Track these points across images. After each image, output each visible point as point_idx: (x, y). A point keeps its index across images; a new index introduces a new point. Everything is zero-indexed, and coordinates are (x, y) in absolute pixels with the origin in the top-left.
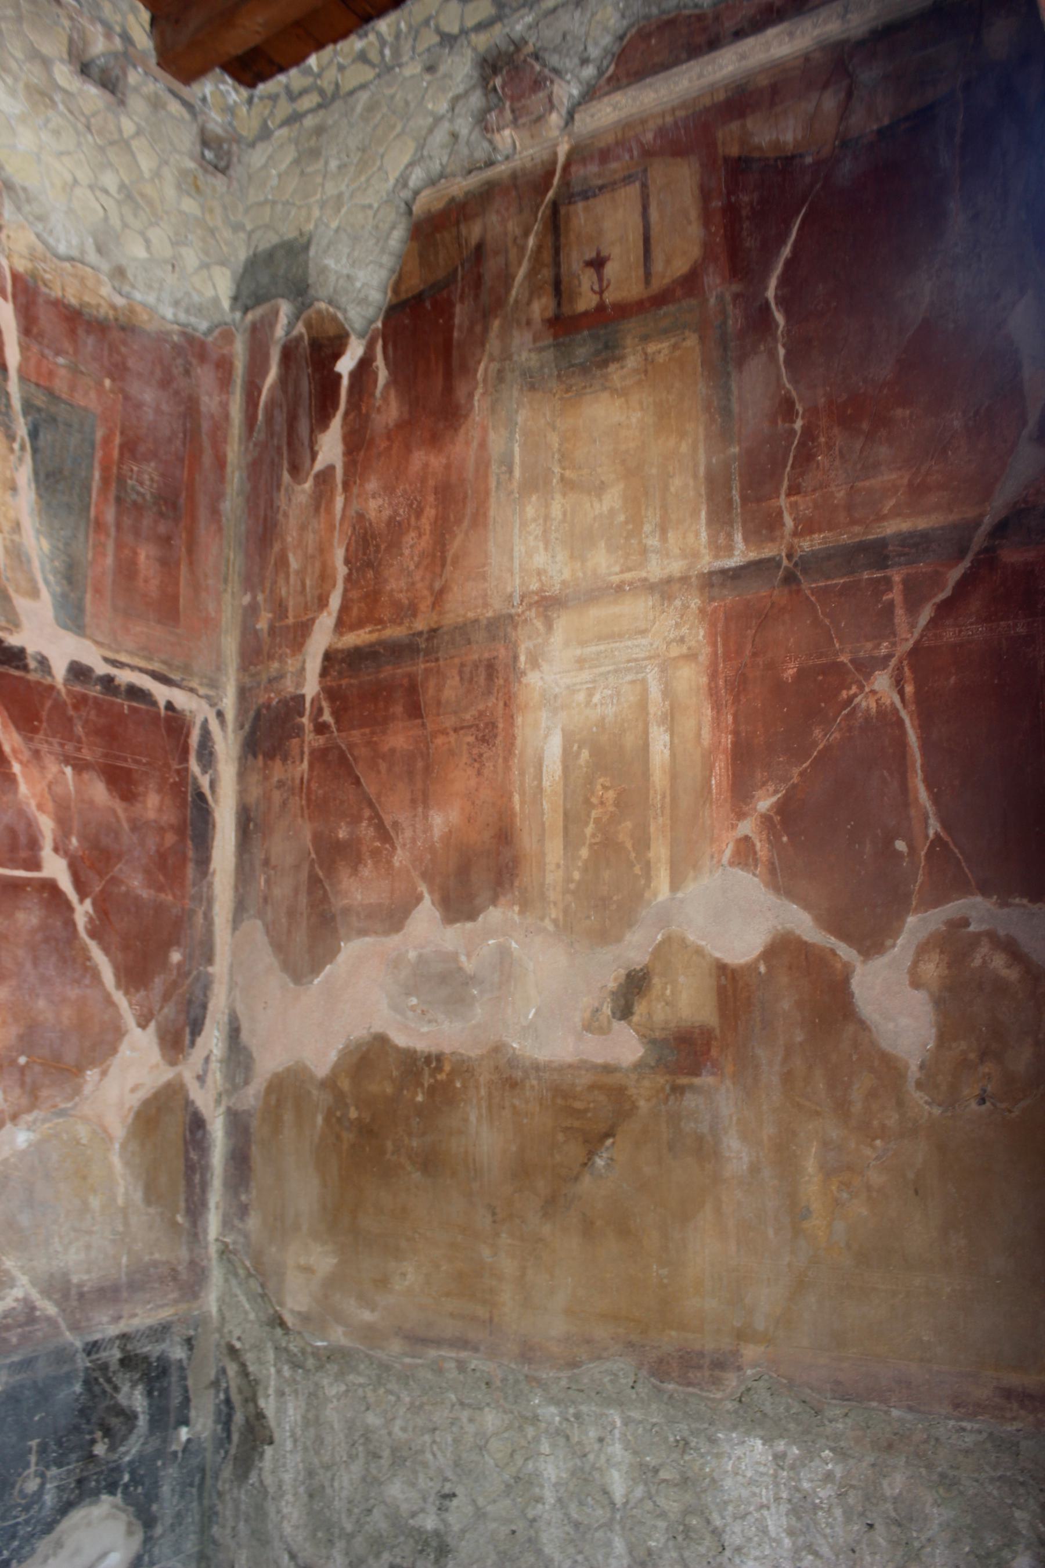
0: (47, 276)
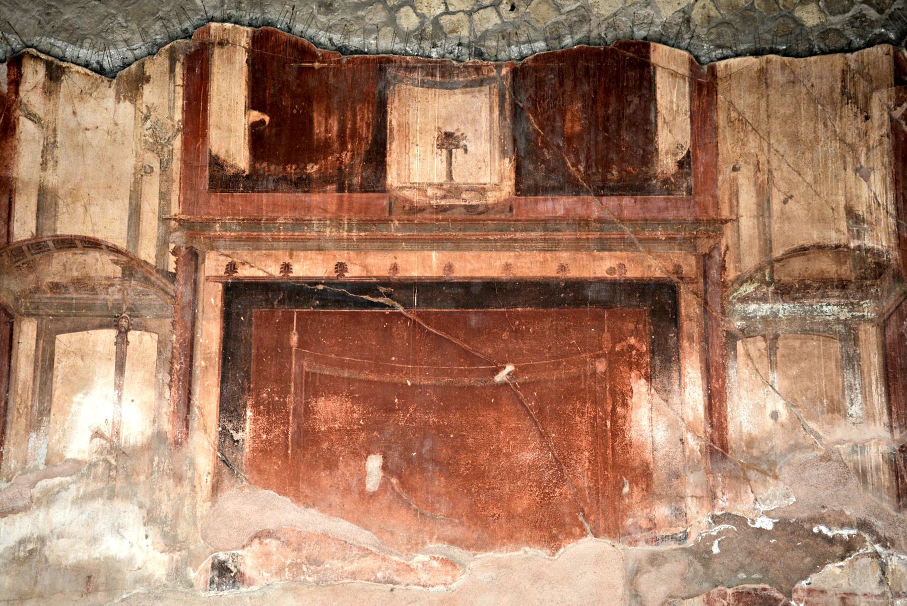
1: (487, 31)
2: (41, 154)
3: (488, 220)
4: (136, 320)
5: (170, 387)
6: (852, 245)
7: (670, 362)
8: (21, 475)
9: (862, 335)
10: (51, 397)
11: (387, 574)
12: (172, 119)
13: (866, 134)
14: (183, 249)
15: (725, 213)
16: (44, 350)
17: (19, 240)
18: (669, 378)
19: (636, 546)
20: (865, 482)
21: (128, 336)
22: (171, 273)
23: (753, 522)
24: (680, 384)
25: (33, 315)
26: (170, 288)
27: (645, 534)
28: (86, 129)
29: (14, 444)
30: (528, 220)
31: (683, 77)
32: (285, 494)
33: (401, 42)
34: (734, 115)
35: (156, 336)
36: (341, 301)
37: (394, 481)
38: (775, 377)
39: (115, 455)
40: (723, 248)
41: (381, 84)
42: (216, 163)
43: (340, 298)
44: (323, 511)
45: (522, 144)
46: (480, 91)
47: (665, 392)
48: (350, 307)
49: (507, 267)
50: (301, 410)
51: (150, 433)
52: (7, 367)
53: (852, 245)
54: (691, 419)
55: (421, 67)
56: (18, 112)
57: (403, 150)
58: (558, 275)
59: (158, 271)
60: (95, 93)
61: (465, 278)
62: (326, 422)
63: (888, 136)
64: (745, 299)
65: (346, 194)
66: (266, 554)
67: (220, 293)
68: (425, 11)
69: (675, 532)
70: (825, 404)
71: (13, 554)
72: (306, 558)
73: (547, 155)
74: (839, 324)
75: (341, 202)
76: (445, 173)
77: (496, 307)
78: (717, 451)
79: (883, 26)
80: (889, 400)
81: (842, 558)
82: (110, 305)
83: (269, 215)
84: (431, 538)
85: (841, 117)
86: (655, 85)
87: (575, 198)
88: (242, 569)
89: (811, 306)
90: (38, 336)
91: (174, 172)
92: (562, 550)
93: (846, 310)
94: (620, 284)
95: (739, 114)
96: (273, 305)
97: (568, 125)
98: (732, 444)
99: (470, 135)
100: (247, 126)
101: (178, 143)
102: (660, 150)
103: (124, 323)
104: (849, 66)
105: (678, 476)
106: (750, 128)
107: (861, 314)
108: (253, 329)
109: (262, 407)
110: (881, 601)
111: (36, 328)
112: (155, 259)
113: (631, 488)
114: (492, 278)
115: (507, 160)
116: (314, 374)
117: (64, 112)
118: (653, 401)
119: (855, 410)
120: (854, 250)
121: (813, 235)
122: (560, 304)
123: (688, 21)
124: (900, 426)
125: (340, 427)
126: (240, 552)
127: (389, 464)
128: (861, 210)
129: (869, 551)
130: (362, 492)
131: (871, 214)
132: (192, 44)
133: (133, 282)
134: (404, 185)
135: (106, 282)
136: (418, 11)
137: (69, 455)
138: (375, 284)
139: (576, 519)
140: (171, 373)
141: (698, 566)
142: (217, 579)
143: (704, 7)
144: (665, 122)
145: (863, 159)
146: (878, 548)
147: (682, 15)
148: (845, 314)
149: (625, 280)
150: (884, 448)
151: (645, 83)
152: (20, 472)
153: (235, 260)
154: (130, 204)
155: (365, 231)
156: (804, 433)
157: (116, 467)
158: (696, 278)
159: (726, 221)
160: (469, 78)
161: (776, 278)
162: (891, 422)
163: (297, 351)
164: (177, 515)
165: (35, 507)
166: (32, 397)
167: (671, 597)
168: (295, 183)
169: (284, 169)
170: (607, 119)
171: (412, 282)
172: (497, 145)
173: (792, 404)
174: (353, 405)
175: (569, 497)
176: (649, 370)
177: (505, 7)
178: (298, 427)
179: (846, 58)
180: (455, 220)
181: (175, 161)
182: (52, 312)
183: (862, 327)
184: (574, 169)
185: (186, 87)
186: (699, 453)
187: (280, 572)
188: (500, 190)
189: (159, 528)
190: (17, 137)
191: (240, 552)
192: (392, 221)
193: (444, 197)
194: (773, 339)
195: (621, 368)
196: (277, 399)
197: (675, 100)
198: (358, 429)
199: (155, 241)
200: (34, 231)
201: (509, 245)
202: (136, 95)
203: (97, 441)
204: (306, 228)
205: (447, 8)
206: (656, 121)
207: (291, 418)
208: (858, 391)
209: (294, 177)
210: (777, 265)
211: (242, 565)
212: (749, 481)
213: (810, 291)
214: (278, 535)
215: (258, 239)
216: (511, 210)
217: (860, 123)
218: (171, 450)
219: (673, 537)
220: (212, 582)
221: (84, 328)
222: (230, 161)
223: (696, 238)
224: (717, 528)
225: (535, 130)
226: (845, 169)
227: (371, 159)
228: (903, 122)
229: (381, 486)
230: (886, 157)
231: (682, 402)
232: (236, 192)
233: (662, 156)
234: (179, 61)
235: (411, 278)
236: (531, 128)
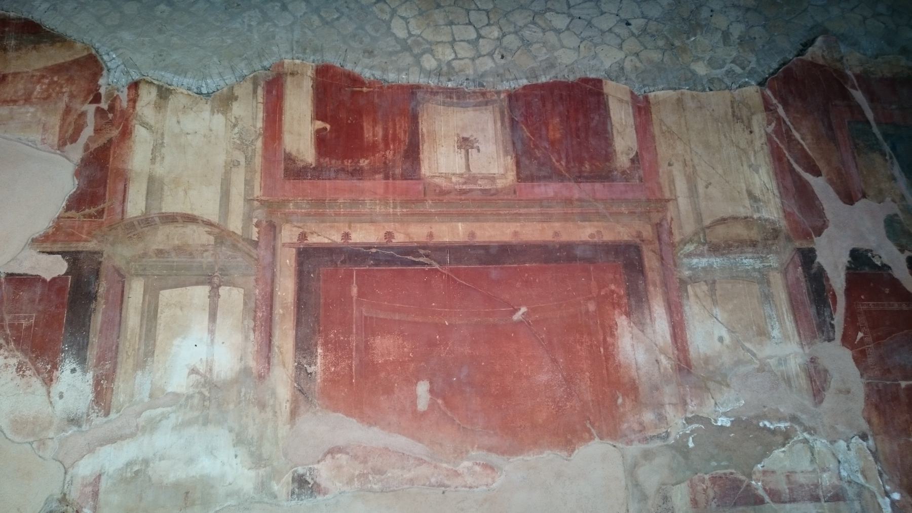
0: (872, 69)
1: (486, 71)
2: (151, 152)
3: (499, 200)
5: (254, 331)
6: (755, 216)
7: (642, 302)
8: (128, 407)
9: (772, 279)
10: (155, 341)
11: (439, 479)
12: (255, 126)
13: (752, 142)
14: (264, 223)
15: (667, 195)
16: (150, 303)
18: (643, 313)
19: (631, 445)
20: (790, 386)
22: (254, 241)
23: (716, 421)
24: (651, 319)
25: (141, 275)
26: (254, 252)
27: (638, 435)
28: (188, 134)
29: (123, 381)
30: (527, 200)
31: (627, 102)
32: (352, 416)
33: (424, 77)
34: (664, 128)
35: (242, 291)
36: (391, 261)
37: (440, 401)
38: (717, 311)
39: (208, 388)
40: (669, 219)
41: (413, 104)
42: (289, 159)
43: (389, 258)
44: (383, 429)
45: (519, 146)
46: (486, 109)
47: (641, 325)
48: (398, 265)
49: (516, 234)
50: (362, 347)
51: (238, 369)
52: (118, 317)
53: (755, 216)
54: (662, 344)
55: (442, 92)
56: (134, 121)
57: (432, 151)
58: (553, 239)
59: (244, 240)
60: (195, 108)
61: (484, 242)
62: (382, 356)
63: (766, 144)
64: (689, 255)
65: (391, 181)
66: (338, 467)
68: (441, 57)
69: (659, 433)
70: (755, 329)
71: (122, 475)
72: (372, 468)
73: (538, 153)
74: (755, 271)
75: (387, 187)
76: (464, 166)
77: (510, 264)
78: (684, 368)
79: (748, 77)
80: (797, 325)
81: (784, 445)
82: (204, 266)
83: (332, 196)
84: (472, 447)
85: (735, 132)
86: (609, 107)
87: (561, 184)
88: (318, 480)
89: (735, 259)
90: (144, 292)
91: (256, 165)
92: (576, 451)
93: (758, 262)
94: (599, 245)
95: (668, 128)
96: (337, 265)
97: (551, 133)
98: (694, 362)
99: (480, 139)
100: (313, 132)
101: (259, 144)
102: (617, 151)
103: (216, 280)
104: (734, 98)
105: (657, 389)
106: (677, 137)
107: (769, 264)
108: (321, 283)
110: (813, 476)
111: (143, 285)
112: (241, 231)
113: (624, 400)
114: (505, 242)
115: (509, 157)
116: (371, 318)
117: (170, 121)
118: (633, 332)
119: (776, 333)
120: (757, 220)
121: (728, 210)
122: (557, 260)
123: (622, 69)
124: (808, 344)
125: (393, 359)
126: (316, 466)
127: (435, 388)
128: (757, 193)
129: (800, 438)
130: (415, 412)
131: (764, 195)
132: (271, 75)
133: (224, 248)
134: (434, 174)
136: (436, 57)
137: (170, 389)
138: (417, 247)
139: (585, 426)
140: (254, 319)
141: (680, 459)
142: (297, 490)
143: (632, 60)
144: (618, 132)
145: (753, 159)
146: (806, 435)
147: (618, 65)
148: (758, 265)
149: (603, 243)
150: (799, 360)
151: (602, 106)
152: (128, 405)
153: (306, 230)
154: (222, 188)
155: (407, 208)
156: (743, 351)
157: (209, 398)
158: (653, 240)
159: (668, 201)
160: (478, 100)
161: (708, 240)
162: (801, 341)
163: (357, 300)
164: (261, 437)
165: (140, 434)
167: (664, 484)
168: (351, 173)
169: (343, 163)
170: (578, 129)
171: (444, 245)
172: (501, 147)
173: (731, 331)
174: (404, 341)
175: (578, 408)
176: (627, 309)
177: (497, 56)
178: (360, 361)
179: (732, 93)
180: (474, 200)
181: (257, 157)
182: (156, 272)
183: (771, 274)
184: (558, 164)
185: (266, 104)
186: (670, 370)
187: (350, 481)
188: (506, 178)
189: (246, 448)
190: (133, 139)
191: (316, 466)
192: (426, 200)
193: (465, 183)
194: (712, 284)
195: (607, 307)
196: (342, 338)
197: (623, 117)
198: (408, 360)
199: (241, 217)
200: (144, 210)
201: (516, 217)
202: (227, 109)
203: (194, 377)
204: (361, 206)
205: (456, 55)
206: (612, 132)
207: (354, 353)
208: (775, 320)
209: (350, 169)
210: (707, 231)
211: (318, 477)
212: (709, 389)
213: (732, 249)
214: (348, 450)
215: (322, 214)
216: (515, 192)
217: (747, 134)
219: (658, 437)
220: (293, 493)
221: (183, 285)
222: (300, 157)
223: (649, 212)
224: (689, 427)
225: (527, 137)
226: (742, 165)
227: (408, 156)
228: (774, 136)
229: (429, 406)
230: (767, 157)
231: (654, 332)
232: (305, 179)
233: (619, 155)
234: (260, 85)
235: (444, 243)
236: (525, 135)
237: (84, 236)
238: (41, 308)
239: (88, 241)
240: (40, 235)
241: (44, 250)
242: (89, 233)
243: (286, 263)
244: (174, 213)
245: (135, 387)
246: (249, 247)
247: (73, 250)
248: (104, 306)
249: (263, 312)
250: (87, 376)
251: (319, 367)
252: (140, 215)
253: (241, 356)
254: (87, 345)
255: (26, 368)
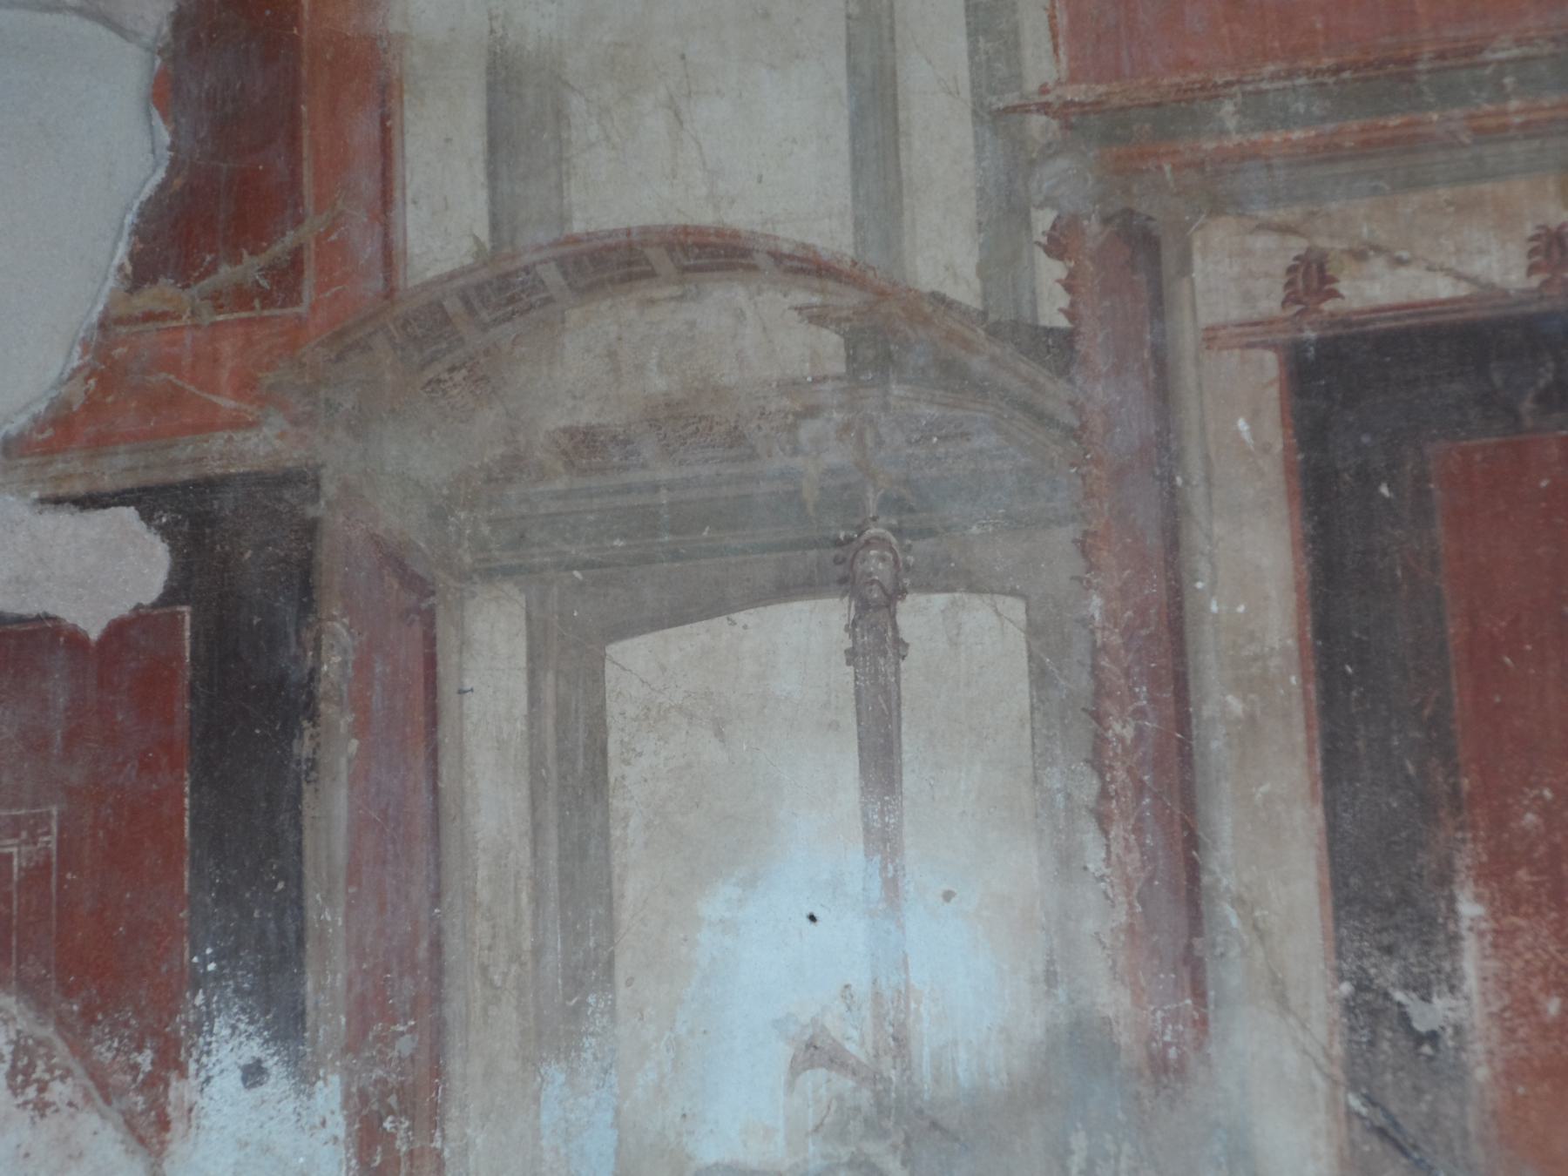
4: (921, 546)
5: (1103, 821)
10: (610, 909)
14: (1093, 226)
17: (430, 275)
21: (902, 620)
22: (1050, 331)
25: (508, 572)
26: (1056, 394)
35: (1016, 609)
39: (898, 1138)
51: (1039, 1033)
59: (994, 332)
67: (1274, 391)
90: (532, 657)
103: (876, 565)
109: (1523, 874)
111: (521, 623)
112: (977, 284)
133: (896, 390)
135: (786, 402)
140: (1098, 763)
153: (1322, 242)
154: (853, 70)
166: (535, 915)
200: (484, 235)
203: (817, 1080)
218: (1137, 1097)
221: (716, 606)
237: (227, 403)
238: (76, 776)
239: (251, 425)
240: (35, 419)
241: (61, 492)
242: (245, 386)
243: (1238, 432)
244: (628, 232)
245: (544, 1143)
246: (1023, 368)
247: (185, 474)
248: (354, 745)
249: (1140, 713)
250: (319, 1099)
251: (1476, 999)
252: (468, 261)
253: (1051, 962)
254: (300, 941)
255: (50, 1070)
